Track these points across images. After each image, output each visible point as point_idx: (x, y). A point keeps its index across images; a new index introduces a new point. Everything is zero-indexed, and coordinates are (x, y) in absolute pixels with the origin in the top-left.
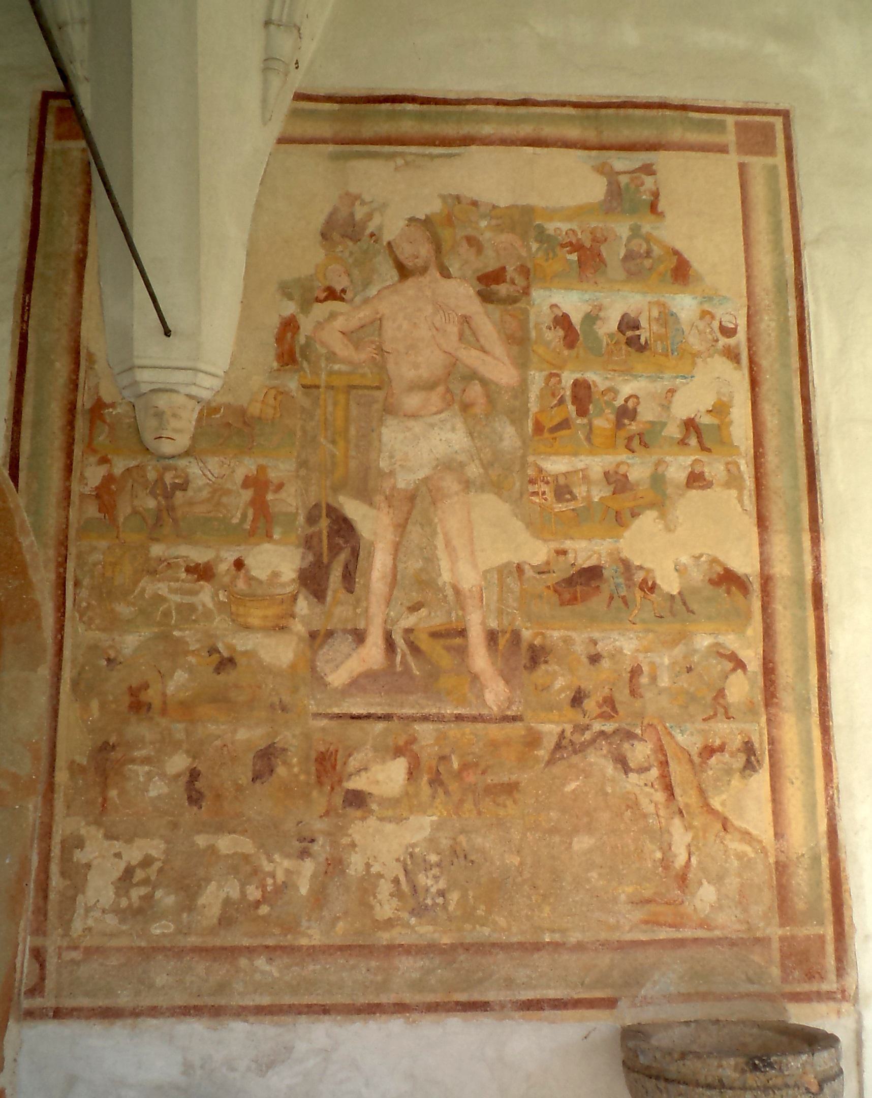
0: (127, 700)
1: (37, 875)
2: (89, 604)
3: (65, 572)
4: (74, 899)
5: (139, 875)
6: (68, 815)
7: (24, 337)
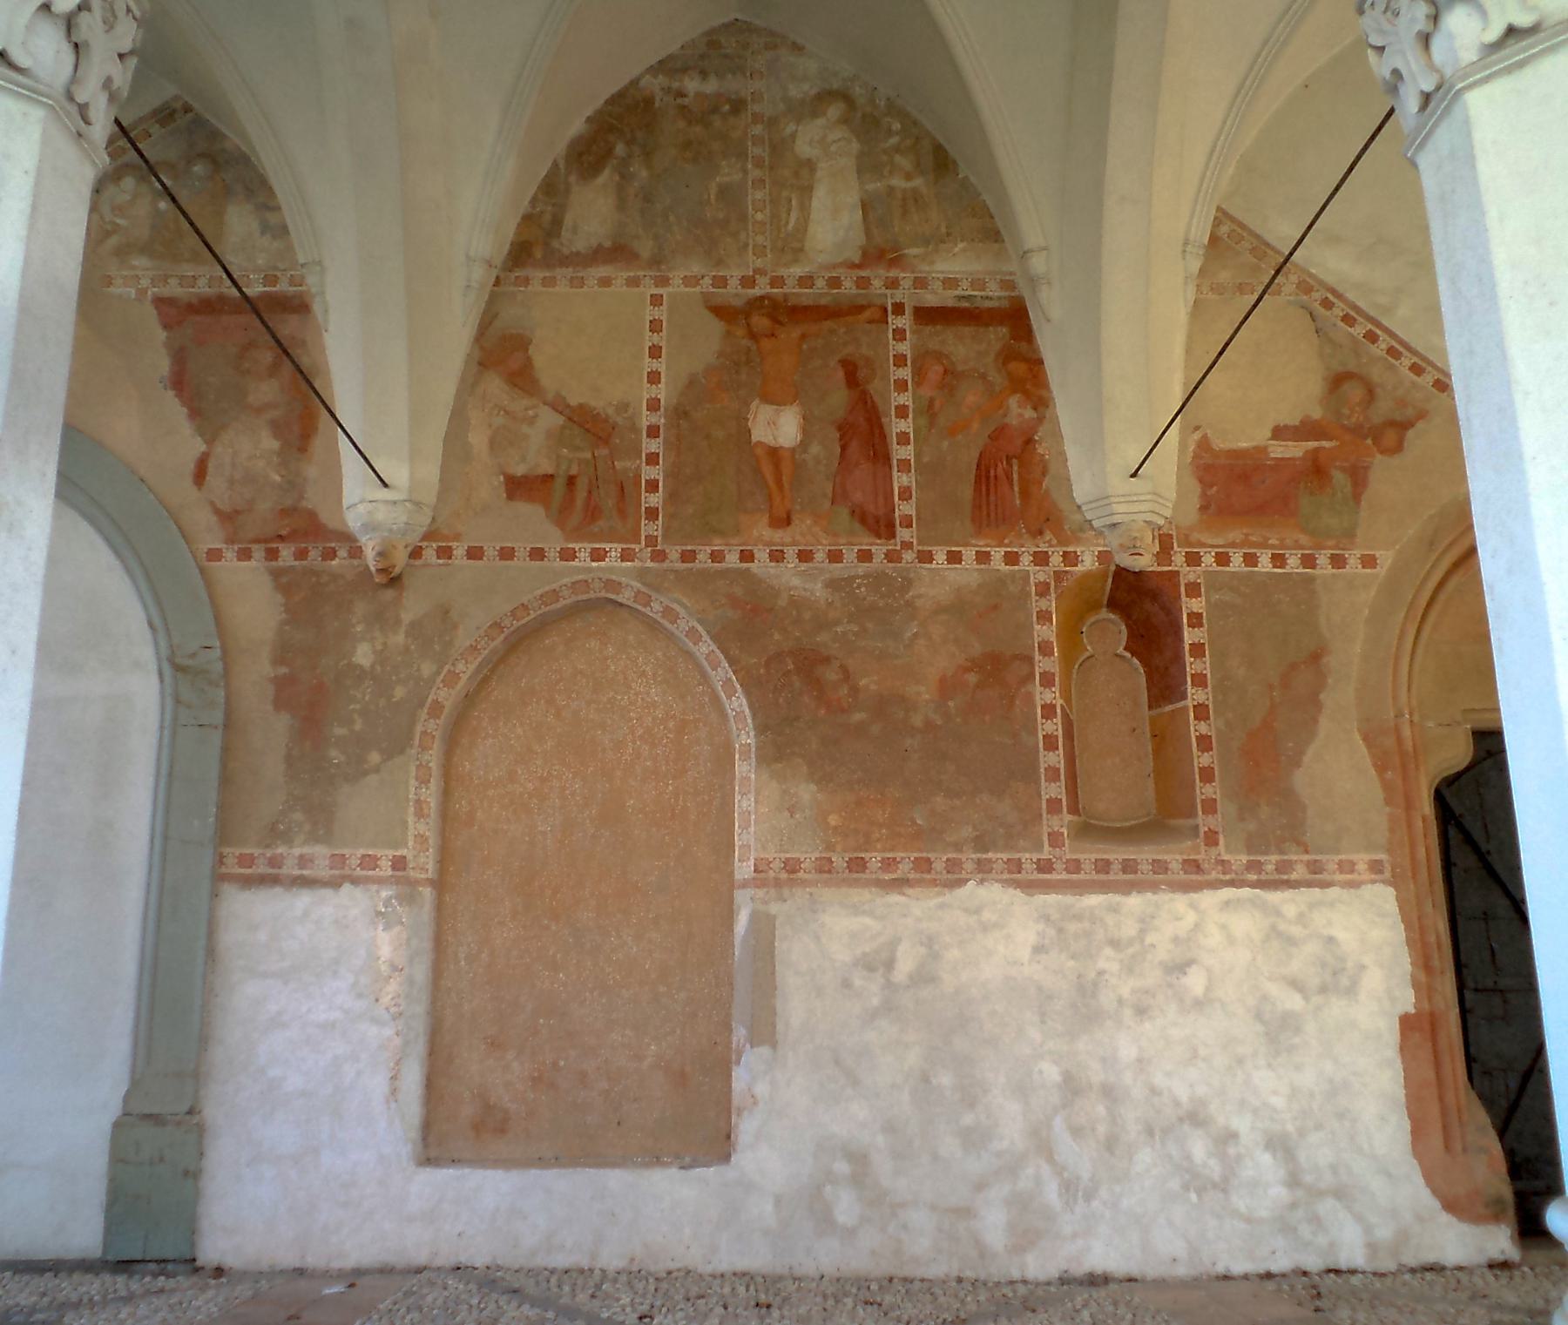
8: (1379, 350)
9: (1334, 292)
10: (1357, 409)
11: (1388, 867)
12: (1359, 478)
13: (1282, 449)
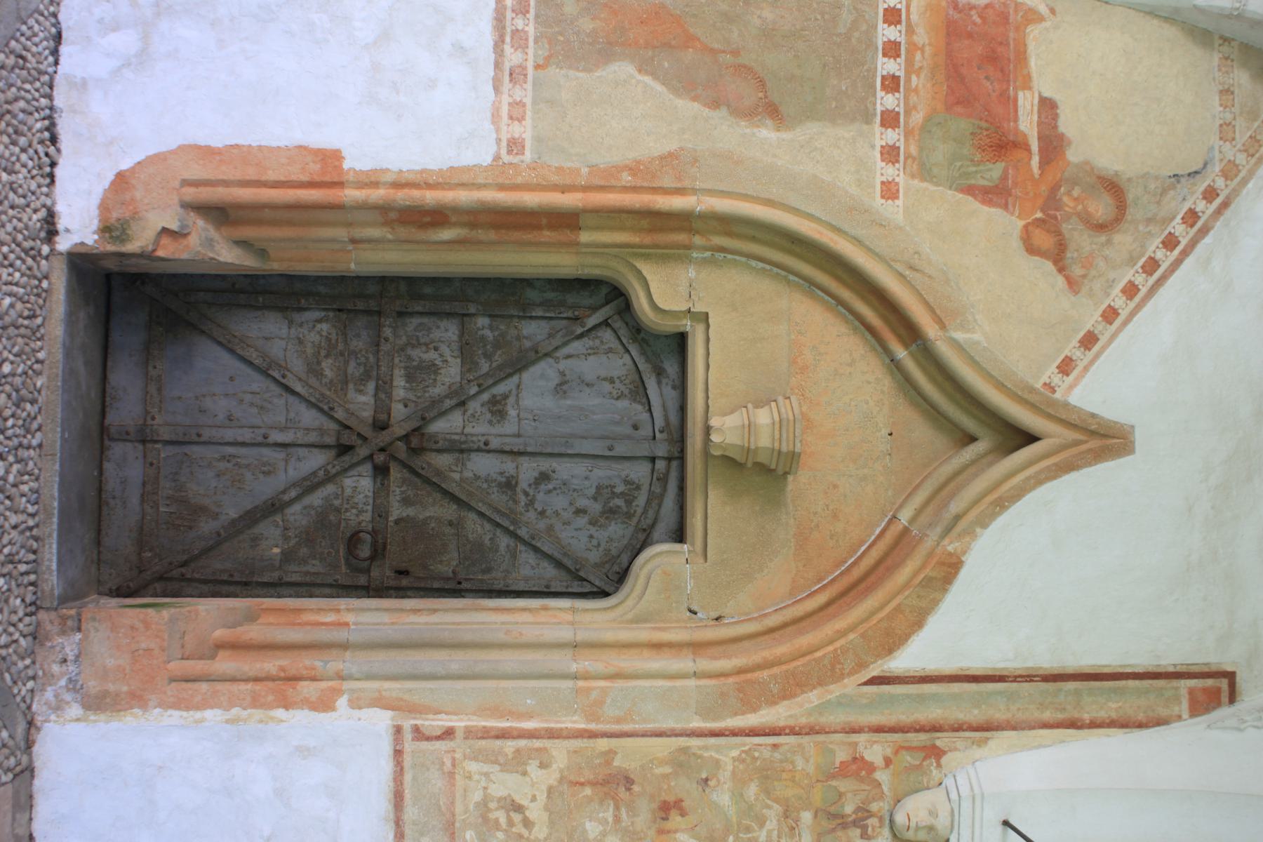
0: (671, 799)
1: (516, 729)
2: (757, 759)
3: (786, 734)
4: (496, 762)
5: (517, 817)
6: (568, 752)
7: (1000, 679)
8: (1154, 247)
9: (1225, 205)
10: (1080, 207)
11: (516, 160)
12: (995, 195)
13: (1029, 107)
